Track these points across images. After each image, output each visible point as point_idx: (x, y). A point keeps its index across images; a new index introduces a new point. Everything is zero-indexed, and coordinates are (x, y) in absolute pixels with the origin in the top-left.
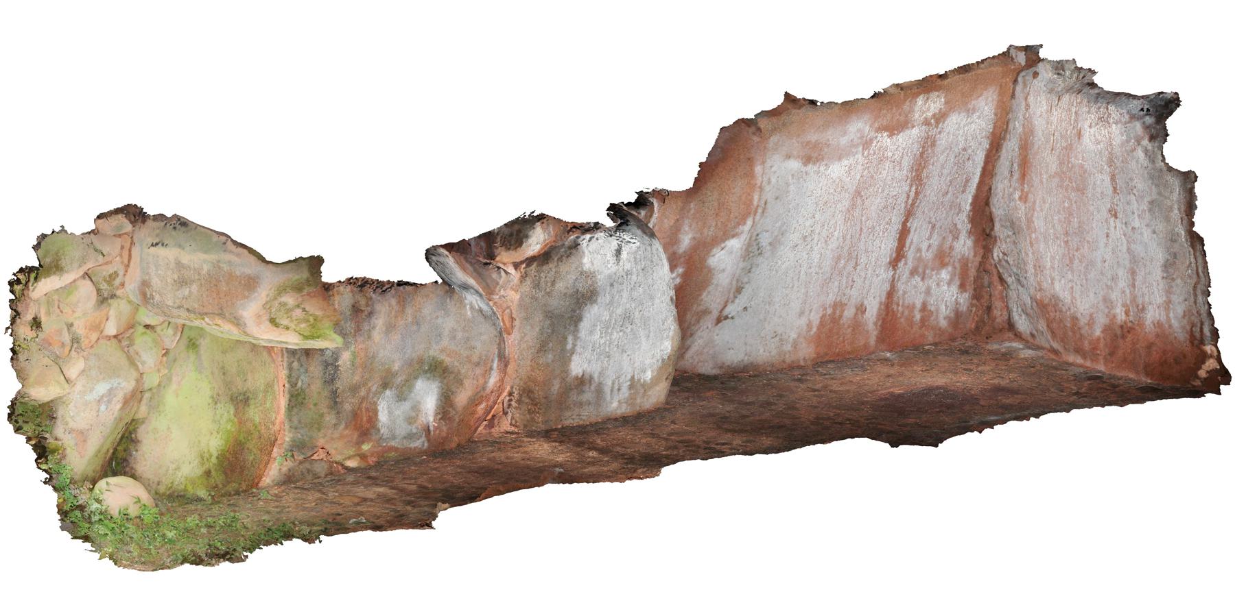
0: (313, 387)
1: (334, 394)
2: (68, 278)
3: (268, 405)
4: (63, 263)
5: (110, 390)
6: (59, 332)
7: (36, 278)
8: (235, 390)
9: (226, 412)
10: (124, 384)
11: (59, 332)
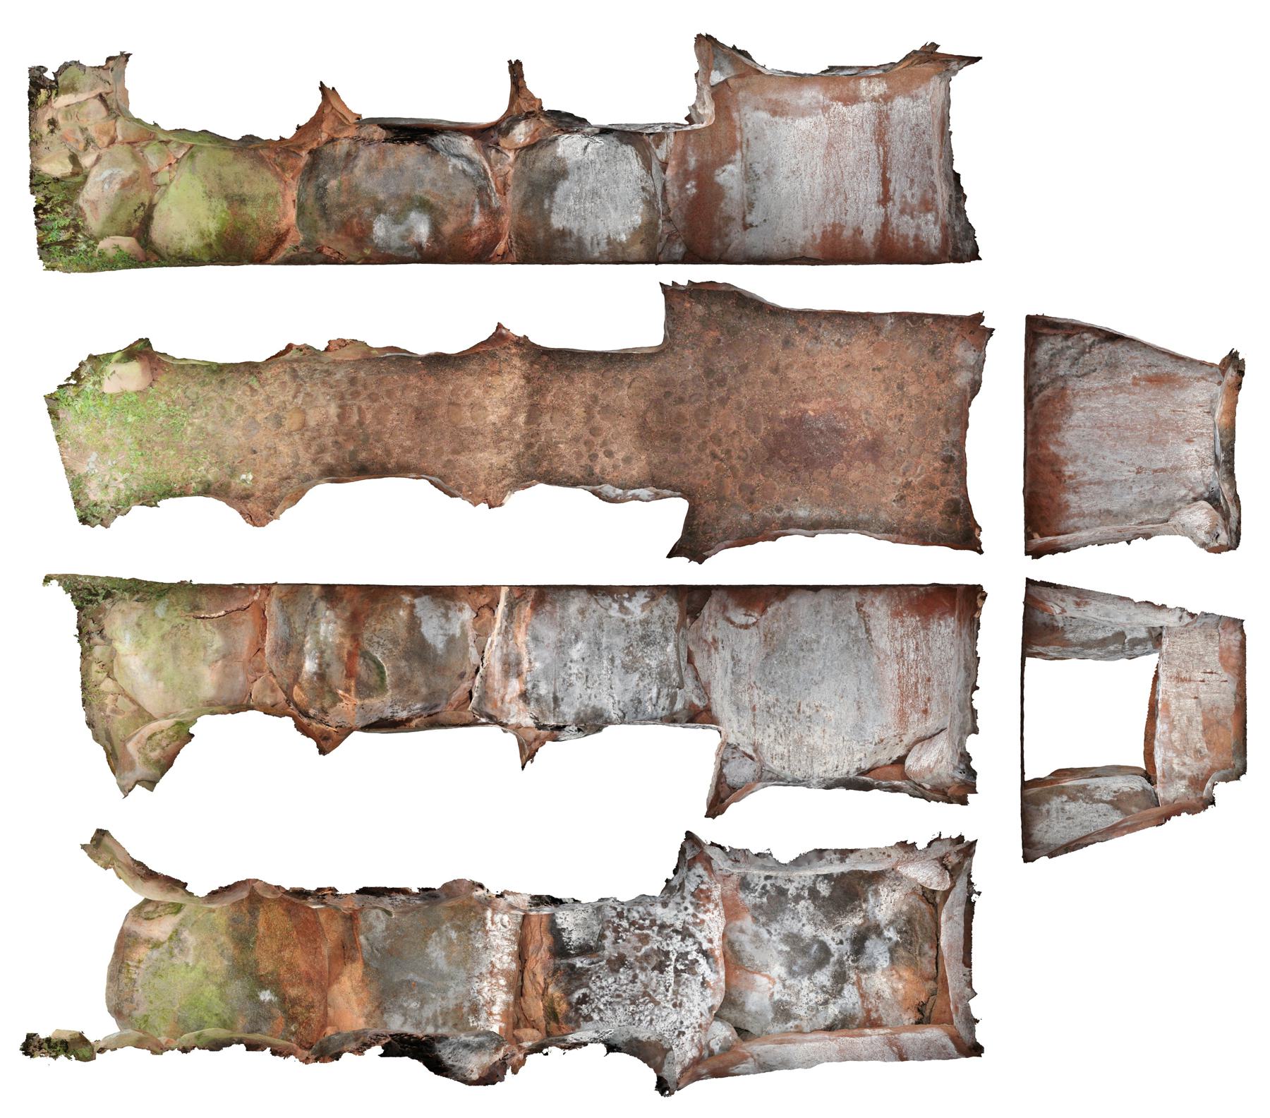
0: (309, 202)
1: (324, 207)
2: (82, 97)
3: (270, 208)
4: (77, 86)
5: (111, 175)
6: (73, 132)
7: (57, 94)
8: (230, 192)
9: (221, 206)
10: (122, 172)
11: (73, 132)
